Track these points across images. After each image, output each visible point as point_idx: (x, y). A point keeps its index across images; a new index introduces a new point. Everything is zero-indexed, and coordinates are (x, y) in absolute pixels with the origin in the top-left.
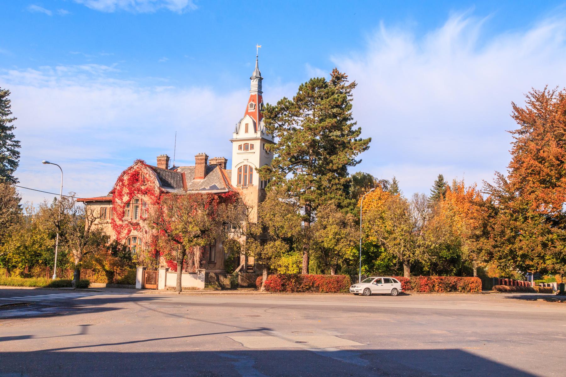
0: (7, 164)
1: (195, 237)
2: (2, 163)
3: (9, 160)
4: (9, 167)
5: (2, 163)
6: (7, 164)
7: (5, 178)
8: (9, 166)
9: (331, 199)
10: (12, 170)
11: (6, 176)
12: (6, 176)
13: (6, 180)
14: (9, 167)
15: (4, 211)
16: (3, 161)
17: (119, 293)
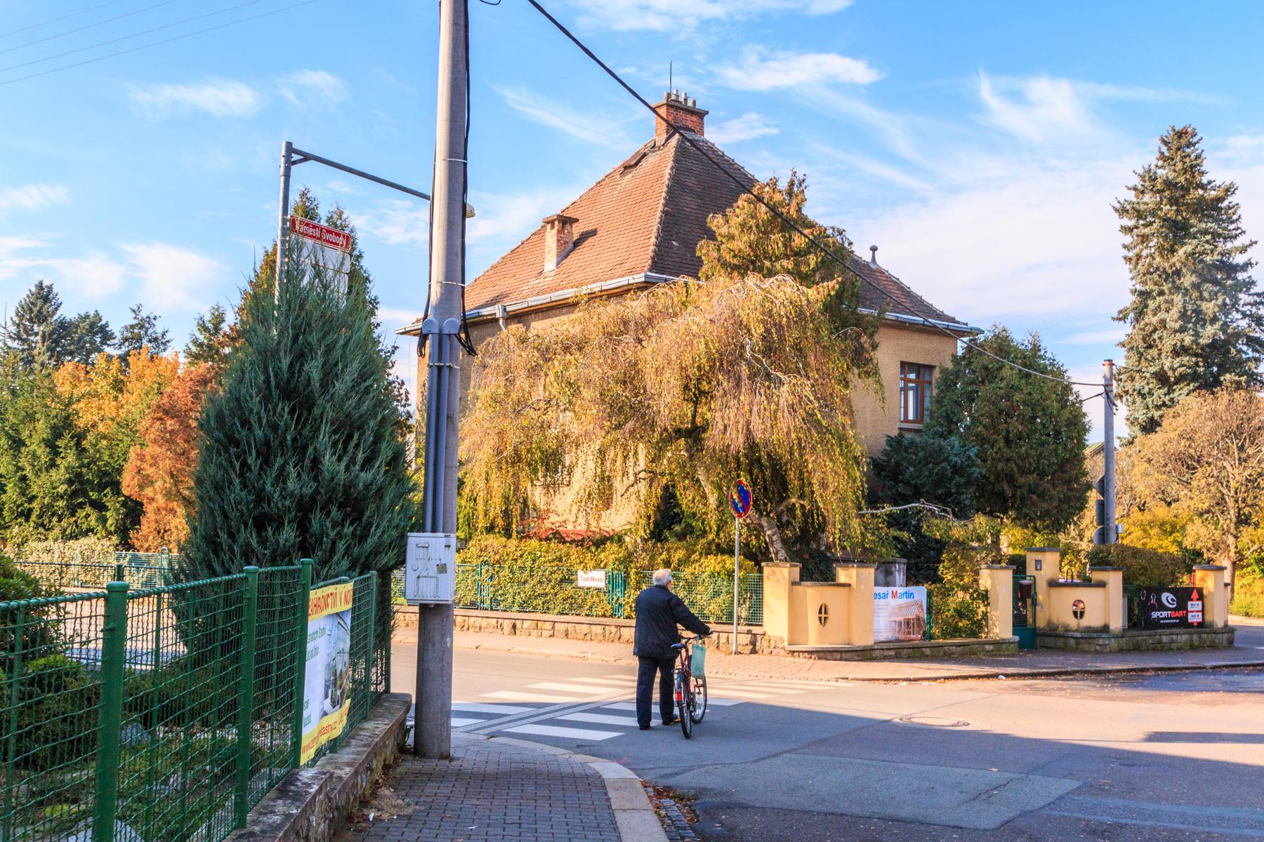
0: (1245, 348)
1: (565, 542)
2: (1235, 347)
3: (1249, 338)
4: (1251, 354)
5: (1235, 347)
6: (1245, 348)
7: (1244, 379)
8: (1250, 351)
9: (817, 331)
10: (1257, 360)
11: (1245, 373)
12: (1245, 373)
13: (1248, 382)
14: (1251, 354)
15: (1251, 451)
16: (1237, 341)
17: (1121, 661)
